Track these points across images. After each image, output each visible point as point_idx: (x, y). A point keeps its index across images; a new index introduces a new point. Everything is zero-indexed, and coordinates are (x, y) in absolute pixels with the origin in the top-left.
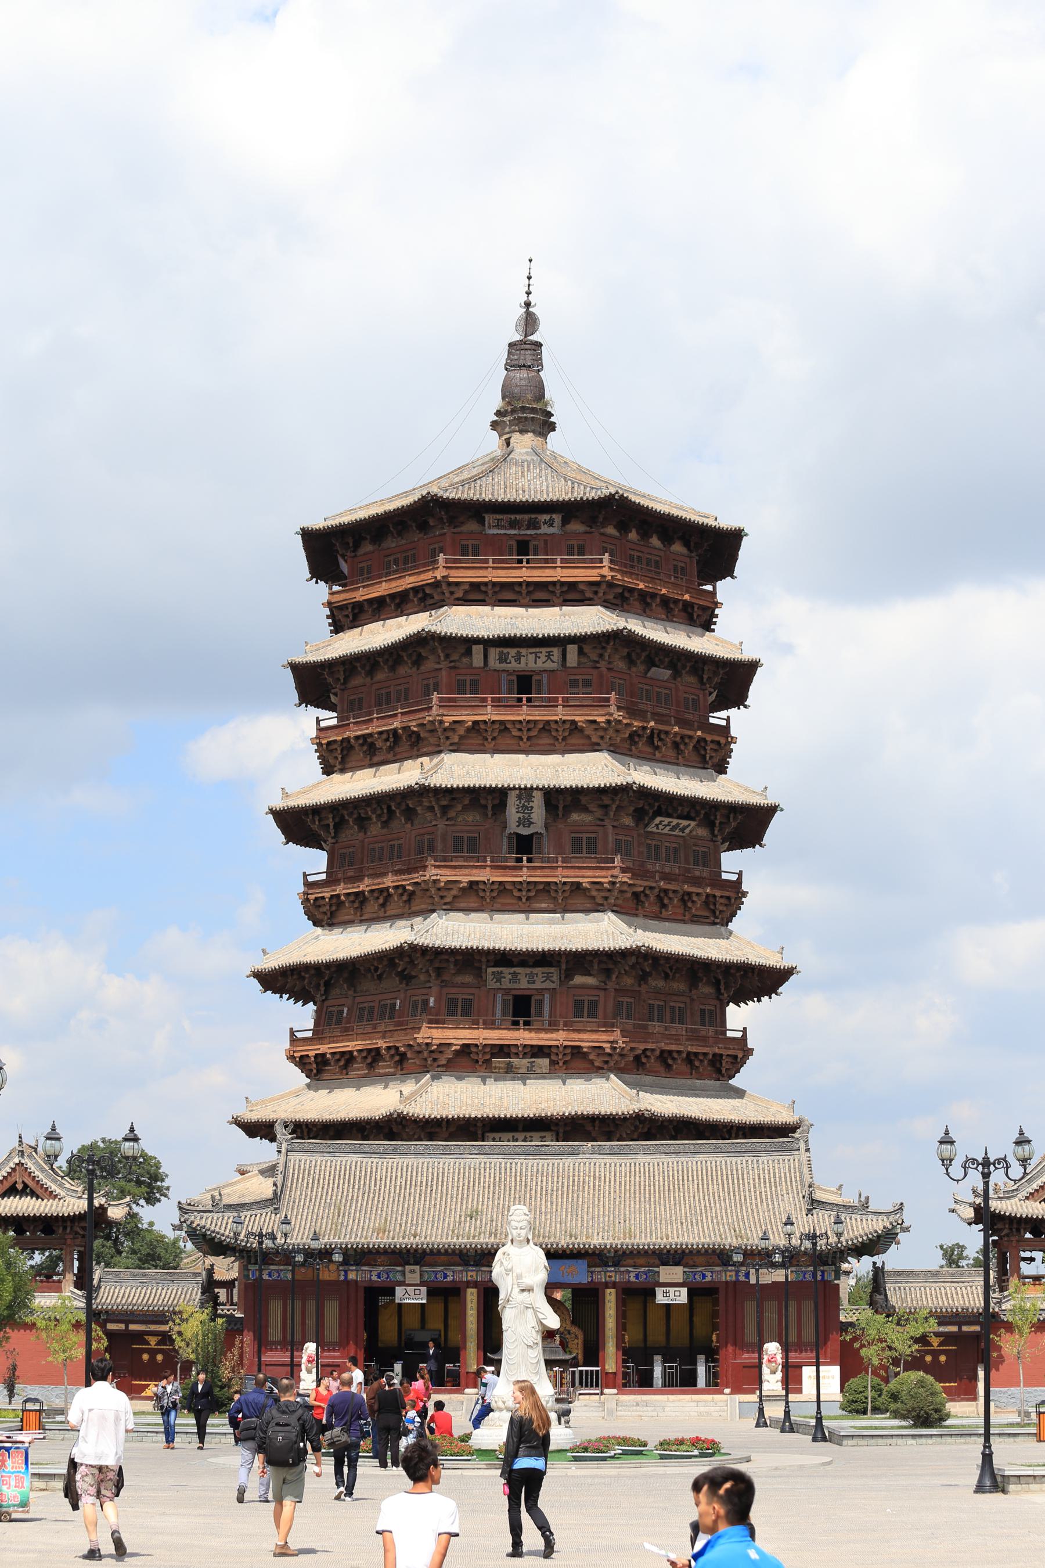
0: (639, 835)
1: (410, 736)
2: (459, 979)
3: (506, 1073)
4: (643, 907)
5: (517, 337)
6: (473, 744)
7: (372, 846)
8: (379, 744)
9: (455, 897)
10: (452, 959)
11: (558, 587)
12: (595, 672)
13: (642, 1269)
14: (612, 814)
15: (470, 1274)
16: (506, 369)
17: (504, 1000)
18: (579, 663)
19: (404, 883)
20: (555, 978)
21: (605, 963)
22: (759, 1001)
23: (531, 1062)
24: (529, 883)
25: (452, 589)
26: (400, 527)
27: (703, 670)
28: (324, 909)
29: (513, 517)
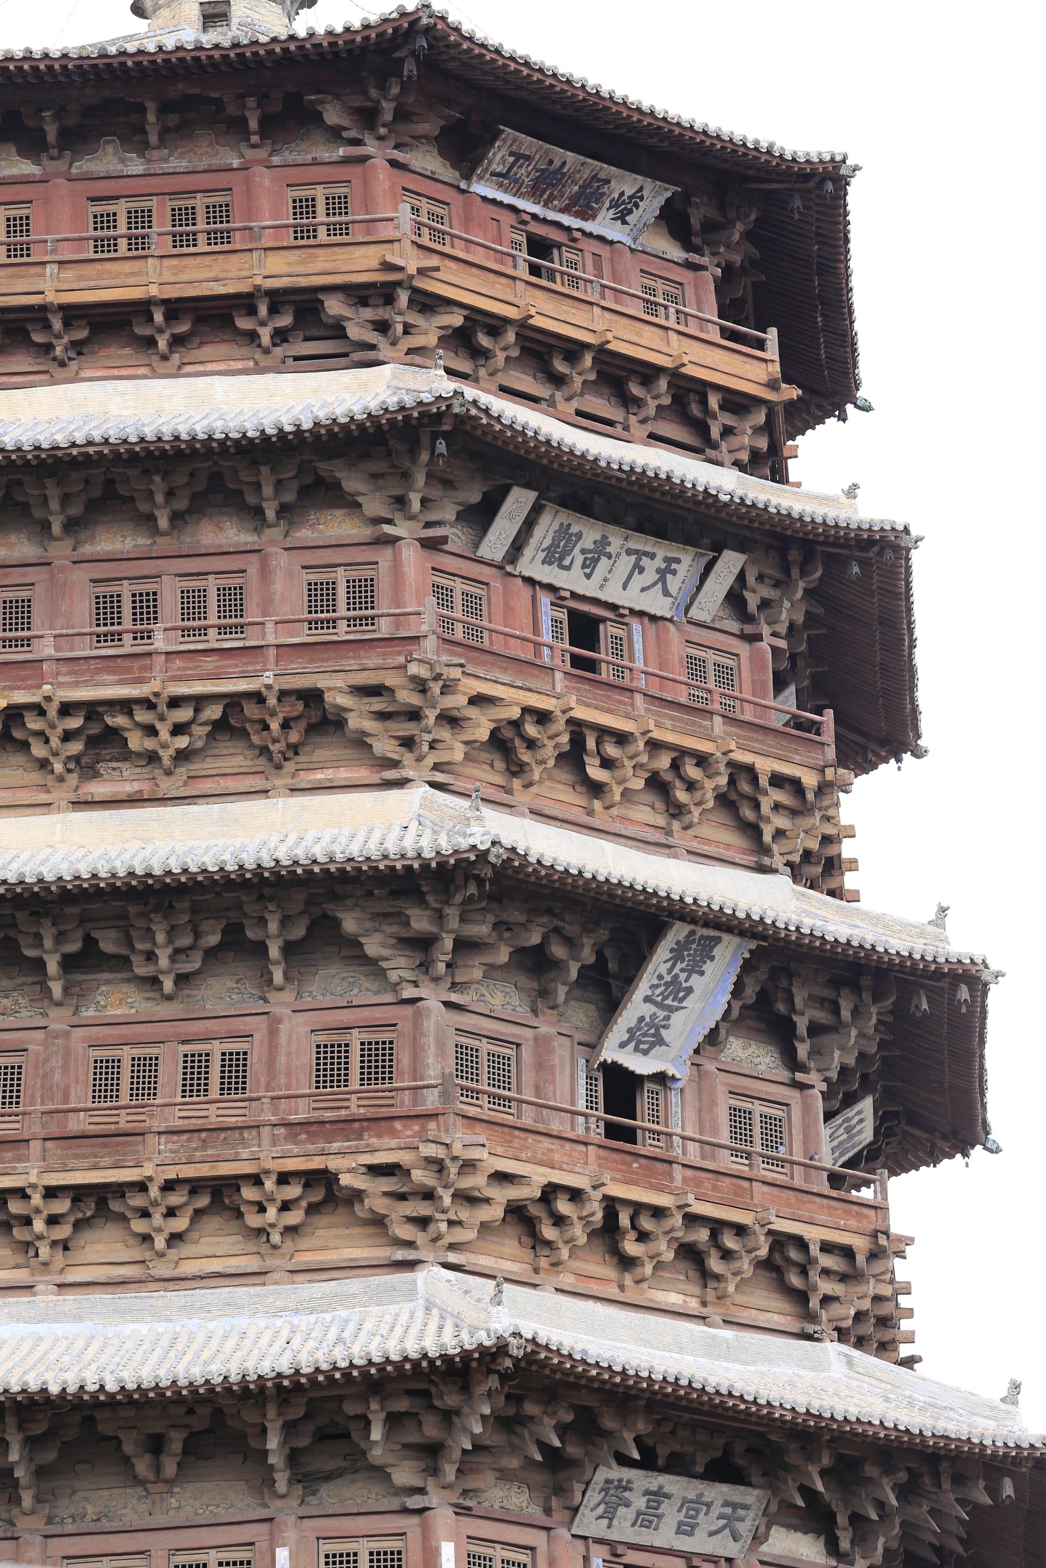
9: (484, 1227)
12: (743, 649)
19: (333, 1164)
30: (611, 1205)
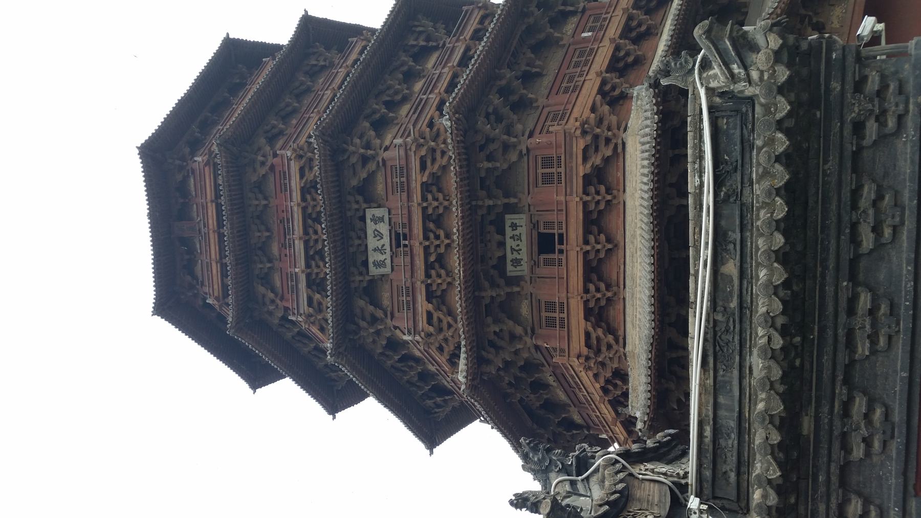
14: (370, 152)
30: (429, 267)
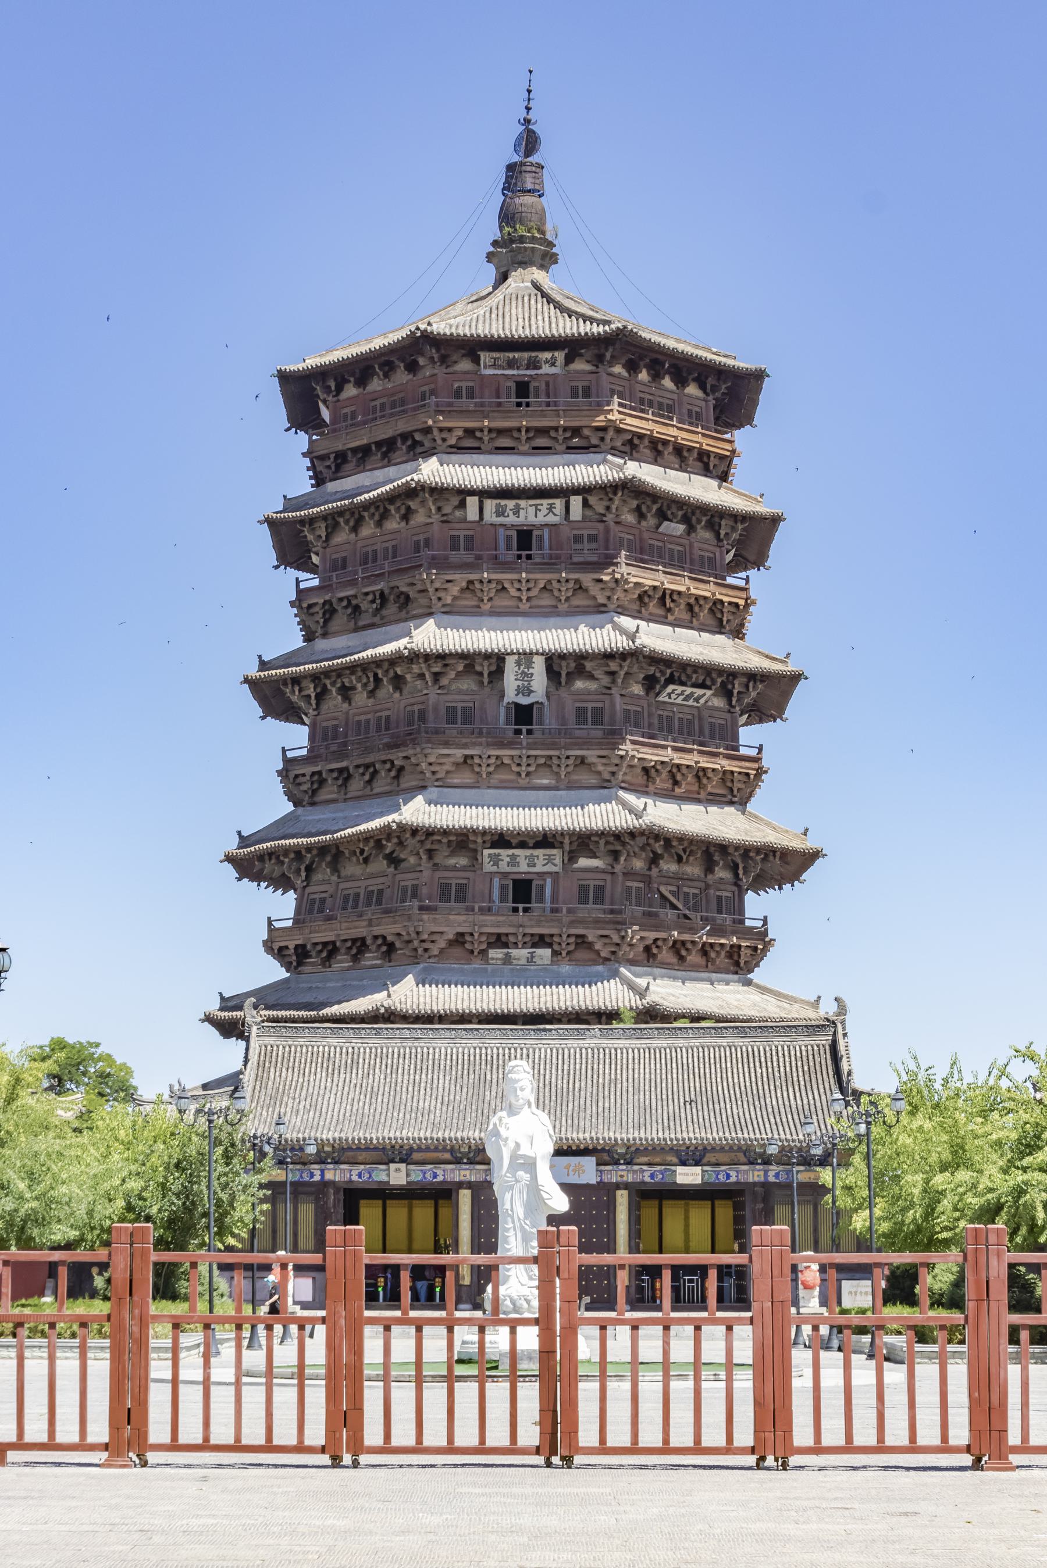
0: (649, 706)
1: (398, 597)
2: (452, 861)
3: (504, 964)
4: (654, 783)
5: (516, 158)
6: (466, 607)
7: (357, 718)
8: (364, 606)
9: (448, 772)
10: (445, 840)
11: (561, 432)
12: (601, 526)
13: (658, 1168)
14: (620, 681)
15: (463, 1173)
16: (504, 194)
17: (503, 888)
18: (583, 514)
20: (558, 861)
21: (612, 844)
22: (780, 888)
23: (531, 953)
24: (528, 757)
25: (445, 435)
26: (386, 368)
27: (720, 525)
28: (305, 787)
29: (511, 355)
30: (498, 757)
